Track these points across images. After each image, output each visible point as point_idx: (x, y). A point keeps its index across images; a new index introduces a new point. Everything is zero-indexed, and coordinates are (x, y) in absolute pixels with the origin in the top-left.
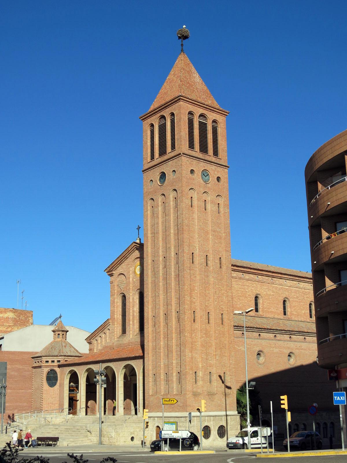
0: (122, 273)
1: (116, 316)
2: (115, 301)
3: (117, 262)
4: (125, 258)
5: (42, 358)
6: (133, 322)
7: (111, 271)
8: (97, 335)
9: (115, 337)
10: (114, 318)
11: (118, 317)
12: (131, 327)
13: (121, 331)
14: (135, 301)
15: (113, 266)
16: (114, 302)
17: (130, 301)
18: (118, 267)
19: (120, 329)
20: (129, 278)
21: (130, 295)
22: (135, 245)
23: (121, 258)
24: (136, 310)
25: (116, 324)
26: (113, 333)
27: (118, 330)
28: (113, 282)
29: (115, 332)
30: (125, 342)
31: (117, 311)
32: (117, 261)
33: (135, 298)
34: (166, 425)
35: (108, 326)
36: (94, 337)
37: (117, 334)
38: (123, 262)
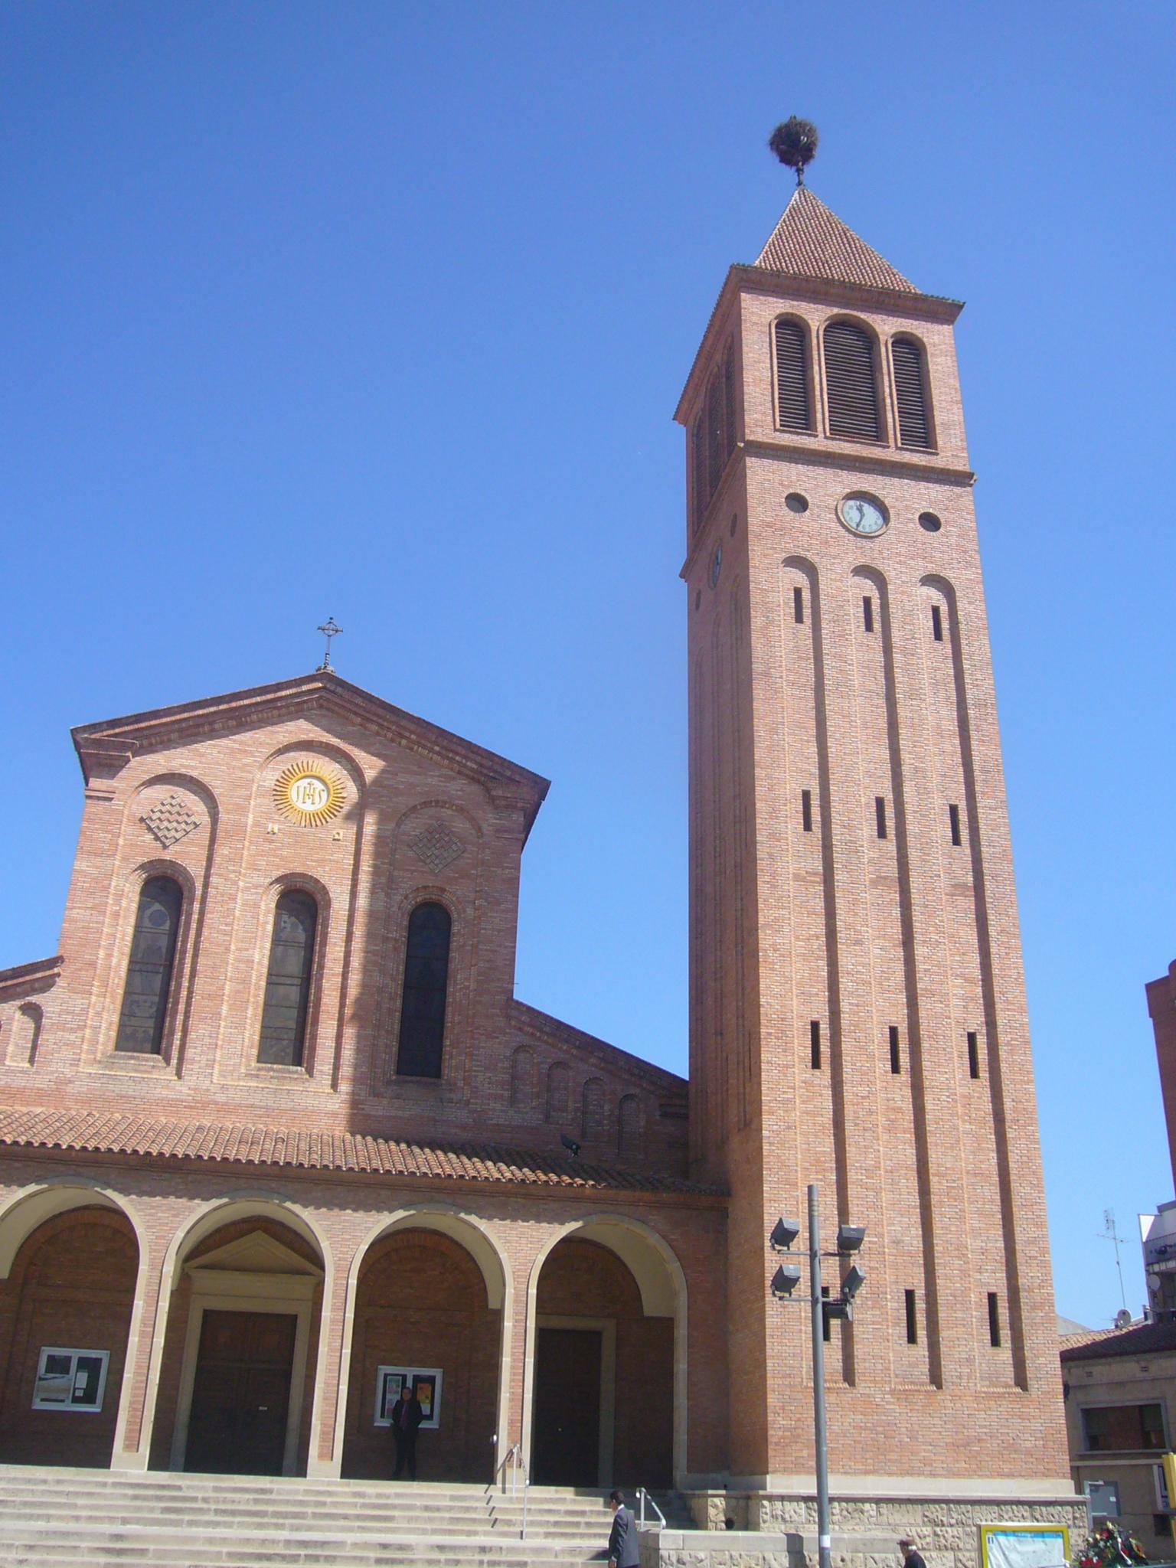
1: (102, 953)
2: (114, 884)
6: (239, 1006)
9: (83, 1056)
10: (93, 964)
11: (114, 961)
12: (222, 1030)
13: (113, 1034)
14: (261, 917)
16: (106, 889)
17: (230, 913)
19: (111, 1024)
20: (243, 810)
21: (235, 883)
24: (260, 963)
25: (95, 990)
26: (73, 1031)
27: (104, 1025)
29: (88, 1031)
30: (165, 1092)
31: (114, 935)
33: (263, 907)
34: (1002, 1538)
37: (94, 1042)
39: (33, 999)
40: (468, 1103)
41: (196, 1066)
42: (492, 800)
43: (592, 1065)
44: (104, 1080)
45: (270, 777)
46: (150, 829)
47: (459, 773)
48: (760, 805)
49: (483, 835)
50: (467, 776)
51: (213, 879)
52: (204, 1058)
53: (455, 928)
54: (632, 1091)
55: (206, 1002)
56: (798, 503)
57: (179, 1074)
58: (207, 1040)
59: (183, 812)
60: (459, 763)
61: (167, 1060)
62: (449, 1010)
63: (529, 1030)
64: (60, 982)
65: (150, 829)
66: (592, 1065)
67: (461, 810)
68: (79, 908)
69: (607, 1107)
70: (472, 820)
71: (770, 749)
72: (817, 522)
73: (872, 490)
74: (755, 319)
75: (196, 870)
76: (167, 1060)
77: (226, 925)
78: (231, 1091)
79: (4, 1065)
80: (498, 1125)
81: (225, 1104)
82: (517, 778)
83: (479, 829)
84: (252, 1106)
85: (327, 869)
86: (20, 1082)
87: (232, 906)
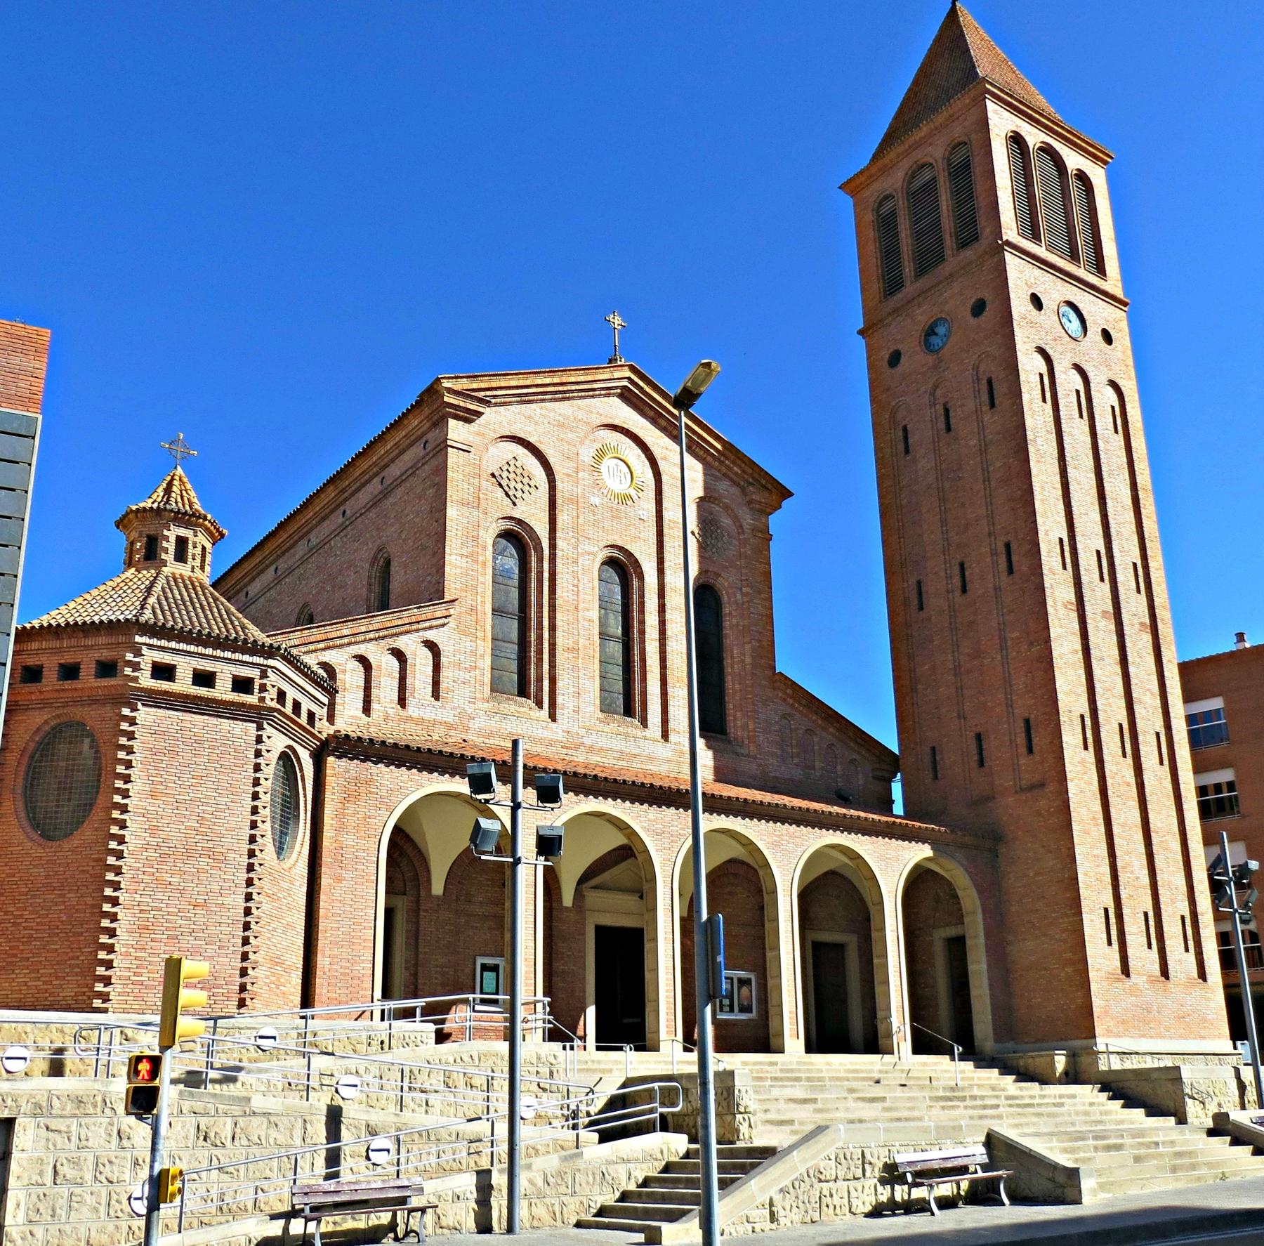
0: (532, 440)
3: (522, 383)
4: (560, 392)
5: (271, 662)
7: (480, 400)
8: (345, 641)
15: (494, 385)
18: (510, 403)
22: (629, 378)
23: (548, 381)
28: (472, 450)
30: (545, 734)
32: (528, 382)
35: (431, 628)
36: (322, 645)
38: (543, 401)
39: (430, 635)
40: (755, 758)
41: (566, 711)
42: (749, 503)
43: (831, 734)
44: (497, 719)
45: (587, 454)
46: (500, 485)
47: (724, 475)
48: (1042, 545)
49: (743, 532)
50: (731, 480)
51: (559, 543)
52: (571, 705)
53: (726, 610)
54: (855, 756)
55: (566, 655)
56: (1037, 302)
57: (553, 717)
58: (572, 689)
59: (524, 475)
60: (727, 466)
61: (539, 704)
62: (728, 679)
63: (791, 701)
64: (452, 622)
65: (500, 485)
66: (831, 734)
67: (726, 508)
68: (457, 554)
69: (839, 768)
70: (736, 519)
71: (1042, 500)
72: (1047, 317)
73: (1080, 306)
74: (997, 132)
75: (542, 531)
76: (539, 704)
77: (574, 586)
78: (594, 736)
79: (414, 697)
80: (776, 777)
81: (591, 747)
82: (770, 487)
83: (741, 526)
84: (611, 750)
85: (638, 544)
86: (429, 714)
87: (575, 569)
